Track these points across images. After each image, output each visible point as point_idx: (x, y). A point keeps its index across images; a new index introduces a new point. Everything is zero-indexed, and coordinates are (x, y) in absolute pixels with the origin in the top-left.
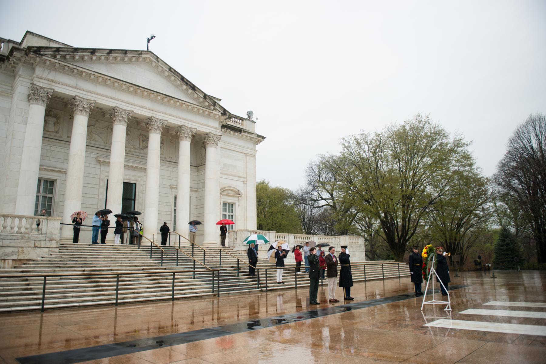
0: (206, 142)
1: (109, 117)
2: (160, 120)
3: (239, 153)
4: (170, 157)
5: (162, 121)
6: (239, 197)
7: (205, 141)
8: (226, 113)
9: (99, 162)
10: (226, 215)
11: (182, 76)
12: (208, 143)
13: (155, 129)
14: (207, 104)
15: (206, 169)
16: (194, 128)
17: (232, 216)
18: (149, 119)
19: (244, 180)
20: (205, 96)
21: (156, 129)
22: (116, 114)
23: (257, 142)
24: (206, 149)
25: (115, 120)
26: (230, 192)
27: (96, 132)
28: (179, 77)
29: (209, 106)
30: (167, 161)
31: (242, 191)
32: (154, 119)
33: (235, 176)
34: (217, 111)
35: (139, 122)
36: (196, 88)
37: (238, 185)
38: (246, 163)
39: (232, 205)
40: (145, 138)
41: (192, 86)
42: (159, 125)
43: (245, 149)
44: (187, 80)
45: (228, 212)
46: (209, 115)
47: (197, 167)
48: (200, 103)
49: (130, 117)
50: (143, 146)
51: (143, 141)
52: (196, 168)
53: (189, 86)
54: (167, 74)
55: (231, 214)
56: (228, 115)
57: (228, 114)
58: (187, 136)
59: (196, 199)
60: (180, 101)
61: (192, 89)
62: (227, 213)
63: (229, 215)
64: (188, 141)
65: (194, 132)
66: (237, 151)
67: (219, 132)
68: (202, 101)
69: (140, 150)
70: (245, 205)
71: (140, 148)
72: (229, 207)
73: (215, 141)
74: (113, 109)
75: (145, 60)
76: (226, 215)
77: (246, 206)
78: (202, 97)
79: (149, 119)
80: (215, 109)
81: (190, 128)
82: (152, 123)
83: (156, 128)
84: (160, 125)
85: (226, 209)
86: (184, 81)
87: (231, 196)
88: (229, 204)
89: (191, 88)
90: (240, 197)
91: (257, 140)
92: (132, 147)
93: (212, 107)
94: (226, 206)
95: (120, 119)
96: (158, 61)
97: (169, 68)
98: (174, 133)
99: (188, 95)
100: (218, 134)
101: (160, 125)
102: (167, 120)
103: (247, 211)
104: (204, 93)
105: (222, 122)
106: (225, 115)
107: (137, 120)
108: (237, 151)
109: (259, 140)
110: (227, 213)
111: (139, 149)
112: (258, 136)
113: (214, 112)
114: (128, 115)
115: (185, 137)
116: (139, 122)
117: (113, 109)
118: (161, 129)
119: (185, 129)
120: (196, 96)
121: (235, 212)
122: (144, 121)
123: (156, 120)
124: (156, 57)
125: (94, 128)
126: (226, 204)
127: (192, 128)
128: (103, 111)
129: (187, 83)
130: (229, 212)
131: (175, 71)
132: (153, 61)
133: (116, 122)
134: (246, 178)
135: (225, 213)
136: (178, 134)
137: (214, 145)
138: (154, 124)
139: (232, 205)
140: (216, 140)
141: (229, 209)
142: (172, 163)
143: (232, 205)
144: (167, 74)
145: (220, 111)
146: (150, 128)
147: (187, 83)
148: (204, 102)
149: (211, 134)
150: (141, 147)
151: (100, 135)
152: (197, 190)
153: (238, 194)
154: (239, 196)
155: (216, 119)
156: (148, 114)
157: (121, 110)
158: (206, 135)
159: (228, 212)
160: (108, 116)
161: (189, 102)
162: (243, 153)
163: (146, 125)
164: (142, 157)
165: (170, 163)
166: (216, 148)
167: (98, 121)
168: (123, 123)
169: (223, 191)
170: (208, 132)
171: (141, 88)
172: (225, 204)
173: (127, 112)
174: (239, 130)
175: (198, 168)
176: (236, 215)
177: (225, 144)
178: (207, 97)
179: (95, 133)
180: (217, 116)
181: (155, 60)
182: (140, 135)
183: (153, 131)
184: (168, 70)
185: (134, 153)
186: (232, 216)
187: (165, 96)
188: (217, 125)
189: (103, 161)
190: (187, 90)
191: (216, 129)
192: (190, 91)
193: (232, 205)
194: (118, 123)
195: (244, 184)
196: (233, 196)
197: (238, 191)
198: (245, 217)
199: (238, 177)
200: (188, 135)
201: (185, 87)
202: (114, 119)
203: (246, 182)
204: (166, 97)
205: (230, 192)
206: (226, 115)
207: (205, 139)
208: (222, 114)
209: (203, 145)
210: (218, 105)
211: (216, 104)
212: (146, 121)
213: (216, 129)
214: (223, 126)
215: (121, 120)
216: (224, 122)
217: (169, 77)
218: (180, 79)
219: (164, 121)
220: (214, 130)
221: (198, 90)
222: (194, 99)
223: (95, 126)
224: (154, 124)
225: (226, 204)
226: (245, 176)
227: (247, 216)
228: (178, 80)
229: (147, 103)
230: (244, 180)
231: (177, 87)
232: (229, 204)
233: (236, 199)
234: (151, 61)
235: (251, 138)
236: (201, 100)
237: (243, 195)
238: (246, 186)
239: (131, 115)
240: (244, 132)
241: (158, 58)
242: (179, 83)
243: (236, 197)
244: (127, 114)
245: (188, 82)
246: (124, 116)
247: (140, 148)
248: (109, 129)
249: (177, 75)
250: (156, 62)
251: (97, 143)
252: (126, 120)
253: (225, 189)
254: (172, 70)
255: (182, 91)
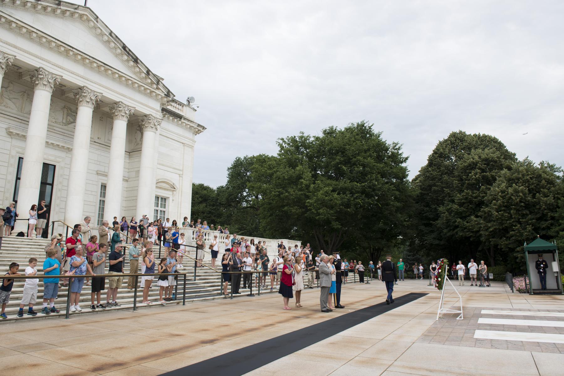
0: (144, 125)
1: (29, 80)
2: (95, 92)
3: (177, 142)
4: (98, 138)
5: (96, 93)
6: (173, 191)
7: (143, 123)
8: (170, 95)
9: (10, 134)
10: (157, 211)
11: (124, 44)
12: (146, 126)
13: (87, 102)
14: (149, 81)
15: (142, 155)
16: (133, 107)
17: (164, 212)
18: (80, 88)
19: (181, 173)
20: (148, 72)
21: (88, 102)
22: (40, 76)
23: (197, 132)
24: (142, 134)
25: (37, 84)
26: (164, 185)
27: (8, 96)
28: (120, 44)
29: (152, 83)
30: (95, 142)
31: (177, 185)
32: (87, 89)
33: (170, 167)
34: (160, 91)
35: (65, 92)
36: (139, 61)
37: (173, 178)
38: (184, 154)
39: (165, 199)
40: (69, 111)
41: (135, 58)
42: (92, 98)
43: (184, 138)
44: (130, 50)
45: (161, 207)
46: (151, 94)
47: (129, 153)
48: (141, 79)
49: (58, 83)
50: (66, 121)
51: (68, 115)
52: (128, 154)
53: (131, 58)
54: (107, 39)
55: (163, 209)
56: (171, 97)
57: (172, 96)
58: (124, 114)
59: (126, 189)
60: (120, 73)
61: (133, 62)
62: (159, 209)
63: (161, 211)
64: (124, 120)
65: (133, 111)
66: (174, 140)
67: (159, 115)
68: (144, 76)
69: (63, 125)
70: (180, 201)
71: (63, 123)
72: (162, 201)
73: (155, 125)
74: (36, 70)
75: (81, 18)
76: (157, 211)
77: (181, 202)
78: (145, 72)
79: (80, 88)
80: (158, 88)
81: (128, 106)
82: (84, 94)
83: (89, 100)
84: (93, 98)
85: (158, 204)
86: (126, 51)
87: (165, 189)
88: (162, 198)
89: (133, 60)
90: (175, 191)
91: (197, 130)
92: (54, 120)
93: (155, 86)
94: (158, 201)
95: (45, 83)
96: (97, 22)
97: (110, 32)
98: (107, 109)
99: (129, 67)
100: (158, 117)
101: (93, 98)
102: (102, 94)
103: (181, 207)
104: (147, 68)
105: (163, 104)
106: (169, 97)
107: (63, 88)
108: (174, 140)
109: (199, 130)
110: (159, 209)
111: (62, 124)
112: (199, 125)
113: (157, 92)
114: (55, 80)
115: (122, 115)
116: (65, 92)
117: (36, 70)
118: (94, 103)
119: (122, 107)
120: (138, 69)
121: (169, 207)
122: (73, 90)
123: (89, 91)
124: (95, 17)
125: (7, 91)
126: (158, 198)
127: (130, 107)
128: (20, 71)
129: (128, 53)
130: (161, 207)
131: (116, 36)
132: (91, 20)
133: (39, 87)
134: (182, 171)
135: (157, 208)
136: (113, 111)
137: (154, 130)
138: (86, 96)
139: (165, 199)
140: (156, 124)
141: (161, 204)
142: (101, 145)
143: (164, 199)
144: (106, 38)
145: (163, 92)
146: (81, 100)
147: (128, 53)
148: (146, 78)
149: (151, 117)
150: (64, 121)
151: (14, 100)
152: (127, 179)
153: (173, 188)
154: (174, 190)
155: (157, 100)
156: (80, 82)
157: (47, 73)
158: (145, 117)
159: (161, 207)
160: (28, 78)
161: (130, 76)
162: (181, 142)
163: (75, 96)
164: (65, 135)
165: (99, 145)
166: (155, 133)
167: (12, 83)
168: (48, 89)
169: (160, 184)
170: (148, 114)
171: (74, 50)
172: (157, 198)
173: (54, 76)
174: (179, 117)
175: (131, 154)
176: (168, 211)
177: (163, 130)
178: (150, 73)
179: (8, 97)
180: (160, 97)
181: (93, 20)
182: (65, 107)
183: (84, 103)
184: (108, 34)
185: (55, 128)
186: (164, 212)
187: (102, 64)
188: (158, 107)
189: (16, 134)
190: (128, 61)
191: (157, 111)
192: (132, 63)
193: (164, 199)
194: (42, 88)
195: (180, 176)
196: (167, 190)
197: (174, 184)
198: (179, 214)
199: (174, 169)
200: (126, 113)
201: (125, 57)
202: (37, 82)
203: (182, 175)
204: (104, 65)
205: (164, 185)
206: (170, 97)
207: (142, 121)
208: (165, 95)
209: (138, 128)
210: (162, 85)
211: (160, 82)
212: (76, 91)
213: (157, 111)
214: (163, 110)
215: (46, 85)
216: (165, 104)
217: (108, 42)
218: (121, 48)
219: (98, 94)
220: (155, 112)
221: (140, 63)
222: (135, 73)
223: (9, 89)
224: (86, 96)
225: (158, 198)
226: (181, 168)
227: (180, 213)
228: (119, 48)
229: (79, 69)
230: (181, 173)
231: (117, 55)
232: (162, 198)
233: (171, 193)
234: (89, 20)
235: (191, 127)
236: (144, 75)
237: (178, 190)
238: (182, 180)
239: (59, 80)
240: (184, 119)
241: (98, 17)
242: (120, 52)
243: (170, 190)
244: (54, 79)
245: (130, 53)
246: (50, 80)
247: (63, 123)
248: (26, 95)
249: (118, 42)
250: (95, 22)
251: (8, 110)
252: (52, 86)
253: (159, 181)
254: (113, 35)
255: (123, 61)
